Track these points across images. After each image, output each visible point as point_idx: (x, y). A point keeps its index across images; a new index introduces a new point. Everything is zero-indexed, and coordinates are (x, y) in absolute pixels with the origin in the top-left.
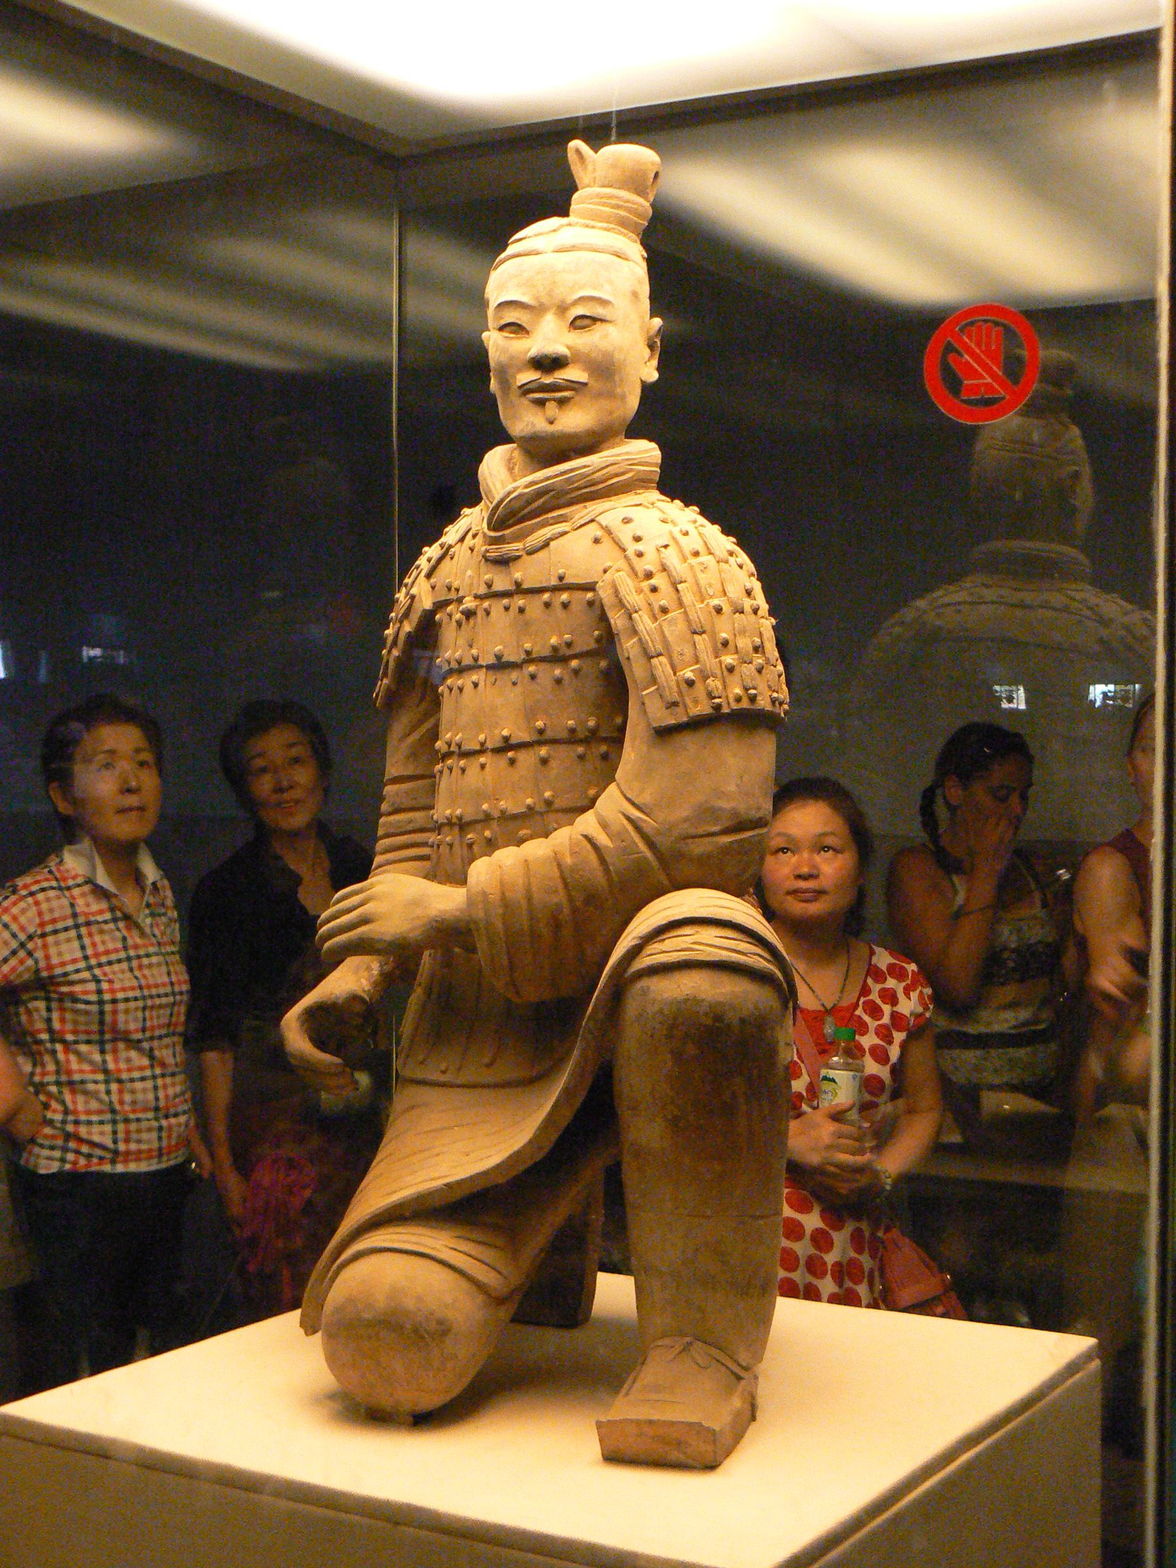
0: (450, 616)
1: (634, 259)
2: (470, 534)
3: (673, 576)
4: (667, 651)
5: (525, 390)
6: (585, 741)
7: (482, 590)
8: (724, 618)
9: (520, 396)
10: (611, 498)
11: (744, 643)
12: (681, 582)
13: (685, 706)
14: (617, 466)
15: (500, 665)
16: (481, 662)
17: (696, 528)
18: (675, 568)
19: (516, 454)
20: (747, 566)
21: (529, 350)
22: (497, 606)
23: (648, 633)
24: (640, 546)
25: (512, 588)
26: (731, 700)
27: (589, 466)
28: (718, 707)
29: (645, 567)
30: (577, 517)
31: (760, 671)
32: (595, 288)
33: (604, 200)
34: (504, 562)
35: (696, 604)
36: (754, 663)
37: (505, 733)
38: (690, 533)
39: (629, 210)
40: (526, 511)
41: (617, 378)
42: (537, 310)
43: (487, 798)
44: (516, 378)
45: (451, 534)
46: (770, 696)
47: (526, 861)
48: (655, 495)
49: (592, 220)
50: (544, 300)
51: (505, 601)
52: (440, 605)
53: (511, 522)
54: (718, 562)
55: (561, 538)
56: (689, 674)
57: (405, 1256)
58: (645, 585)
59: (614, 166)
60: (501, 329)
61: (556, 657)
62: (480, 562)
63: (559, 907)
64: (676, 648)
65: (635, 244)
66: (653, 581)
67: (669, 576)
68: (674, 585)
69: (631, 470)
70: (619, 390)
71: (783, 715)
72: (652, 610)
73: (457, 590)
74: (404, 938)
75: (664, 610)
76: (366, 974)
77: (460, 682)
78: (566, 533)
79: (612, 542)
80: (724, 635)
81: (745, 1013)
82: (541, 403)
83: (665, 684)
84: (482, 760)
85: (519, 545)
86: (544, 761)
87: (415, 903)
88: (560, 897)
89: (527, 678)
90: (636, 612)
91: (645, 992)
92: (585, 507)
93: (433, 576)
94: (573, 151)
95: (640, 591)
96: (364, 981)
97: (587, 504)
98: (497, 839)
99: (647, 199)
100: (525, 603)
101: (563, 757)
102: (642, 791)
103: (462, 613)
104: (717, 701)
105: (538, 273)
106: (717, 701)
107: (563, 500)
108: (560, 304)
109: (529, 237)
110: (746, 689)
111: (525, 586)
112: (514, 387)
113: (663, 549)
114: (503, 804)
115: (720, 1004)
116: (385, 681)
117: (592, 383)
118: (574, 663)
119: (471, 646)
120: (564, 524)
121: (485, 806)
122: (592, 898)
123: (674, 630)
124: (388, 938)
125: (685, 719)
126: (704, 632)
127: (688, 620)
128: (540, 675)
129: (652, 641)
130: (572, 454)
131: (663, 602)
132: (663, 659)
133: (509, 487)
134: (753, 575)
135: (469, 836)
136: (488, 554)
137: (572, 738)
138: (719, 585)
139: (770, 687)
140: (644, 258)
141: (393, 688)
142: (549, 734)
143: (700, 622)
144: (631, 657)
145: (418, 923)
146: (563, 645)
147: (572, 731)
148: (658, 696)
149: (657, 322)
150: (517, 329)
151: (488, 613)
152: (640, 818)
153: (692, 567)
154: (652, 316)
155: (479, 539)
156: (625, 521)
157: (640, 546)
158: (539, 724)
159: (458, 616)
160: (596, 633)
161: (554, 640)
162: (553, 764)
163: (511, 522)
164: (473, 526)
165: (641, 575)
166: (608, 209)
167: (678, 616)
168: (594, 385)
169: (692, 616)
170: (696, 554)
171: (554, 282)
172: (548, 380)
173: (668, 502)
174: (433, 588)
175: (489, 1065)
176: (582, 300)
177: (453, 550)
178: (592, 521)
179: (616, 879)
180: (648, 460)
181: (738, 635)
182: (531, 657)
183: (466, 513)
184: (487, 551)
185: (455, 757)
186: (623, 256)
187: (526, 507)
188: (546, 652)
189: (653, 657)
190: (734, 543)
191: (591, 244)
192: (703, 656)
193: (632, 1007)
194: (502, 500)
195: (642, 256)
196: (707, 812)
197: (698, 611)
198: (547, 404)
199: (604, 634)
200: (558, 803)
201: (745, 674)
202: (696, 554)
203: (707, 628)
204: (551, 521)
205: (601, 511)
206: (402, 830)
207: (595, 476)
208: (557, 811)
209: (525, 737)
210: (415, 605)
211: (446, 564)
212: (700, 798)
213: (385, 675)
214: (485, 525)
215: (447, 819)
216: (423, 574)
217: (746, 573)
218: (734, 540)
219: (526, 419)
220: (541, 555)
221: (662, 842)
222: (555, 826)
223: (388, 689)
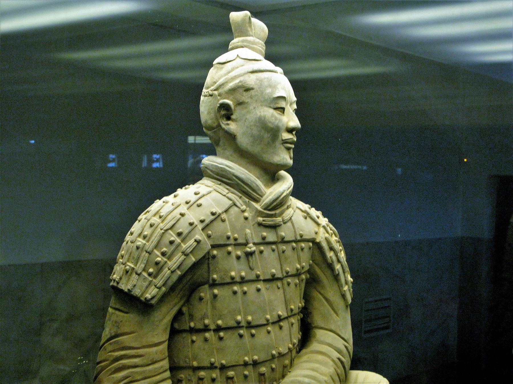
5: (285, 142)
9: (281, 144)
15: (273, 279)
34: (274, 227)
43: (274, 348)
51: (274, 247)
73: (236, 239)
111: (286, 239)
112: (280, 138)
151: (261, 252)
159: (239, 253)
194: (280, 196)
206: (157, 373)
211: (218, 225)
216: (200, 227)
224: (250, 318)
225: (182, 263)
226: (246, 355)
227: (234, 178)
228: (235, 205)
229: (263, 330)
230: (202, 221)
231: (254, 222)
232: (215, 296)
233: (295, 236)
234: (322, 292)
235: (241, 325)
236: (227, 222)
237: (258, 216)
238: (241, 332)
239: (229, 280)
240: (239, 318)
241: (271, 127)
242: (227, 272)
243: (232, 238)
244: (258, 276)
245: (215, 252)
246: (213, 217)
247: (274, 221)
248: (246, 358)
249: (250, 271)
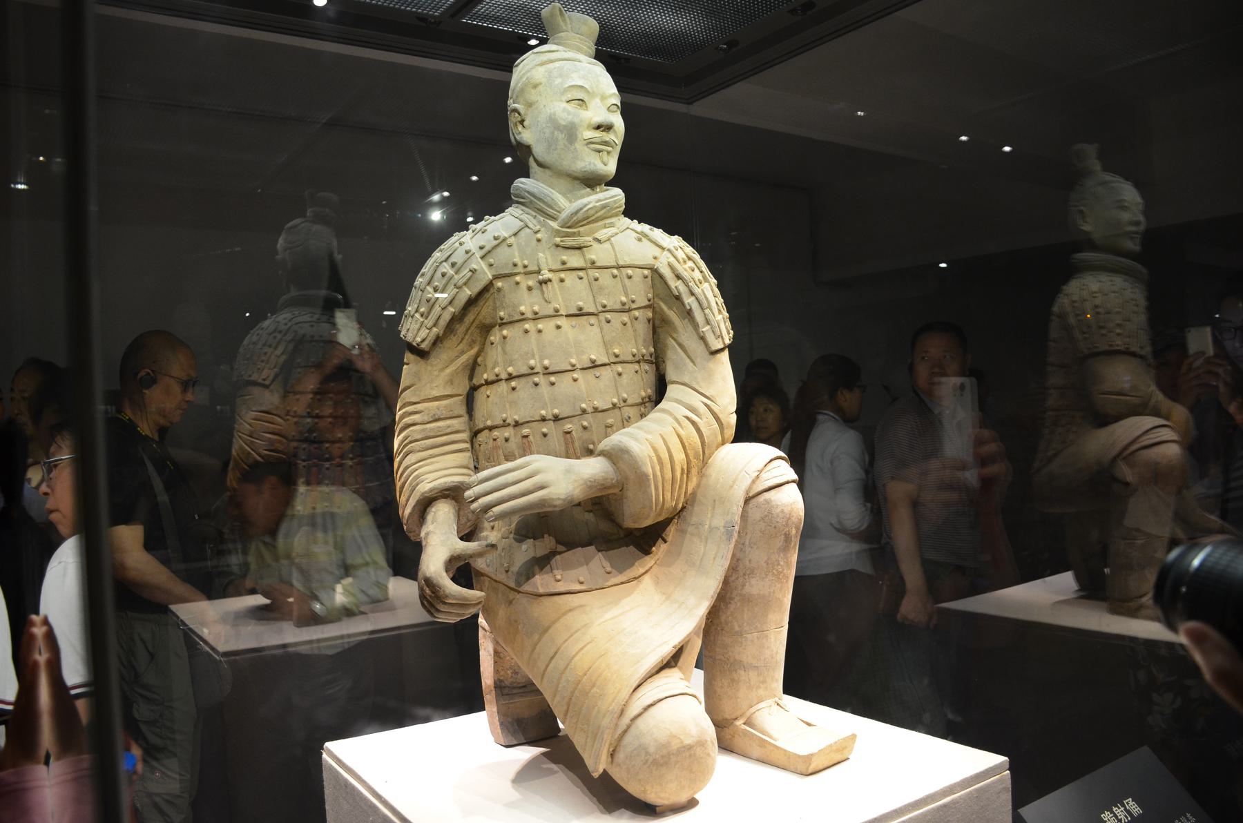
5: (590, 142)
6: (638, 362)
7: (558, 266)
15: (580, 313)
22: (570, 278)
37: (593, 357)
43: (584, 401)
51: (581, 273)
52: (497, 277)
61: (624, 309)
73: (525, 267)
78: (617, 234)
82: (599, 151)
91: (768, 502)
98: (591, 426)
111: (598, 264)
116: (435, 329)
124: (563, 497)
128: (612, 321)
142: (621, 358)
144: (693, 308)
145: (576, 484)
151: (562, 281)
159: (530, 283)
162: (624, 376)
164: (531, 225)
178: (628, 228)
184: (562, 241)
188: (618, 306)
194: (581, 209)
200: (630, 401)
204: (607, 226)
206: (441, 433)
208: (628, 406)
211: (503, 252)
216: (478, 254)
220: (607, 245)
224: (546, 362)
225: (454, 298)
226: (543, 409)
227: (527, 194)
228: (527, 226)
229: (568, 376)
230: (481, 248)
231: (550, 245)
232: (505, 338)
234: (675, 335)
235: (535, 371)
236: (515, 246)
237: (555, 237)
238: (536, 379)
239: (517, 317)
240: (532, 362)
241: (563, 125)
242: (515, 306)
243: (520, 264)
244: (557, 311)
245: (499, 284)
246: (496, 242)
248: (543, 412)
249: (546, 304)
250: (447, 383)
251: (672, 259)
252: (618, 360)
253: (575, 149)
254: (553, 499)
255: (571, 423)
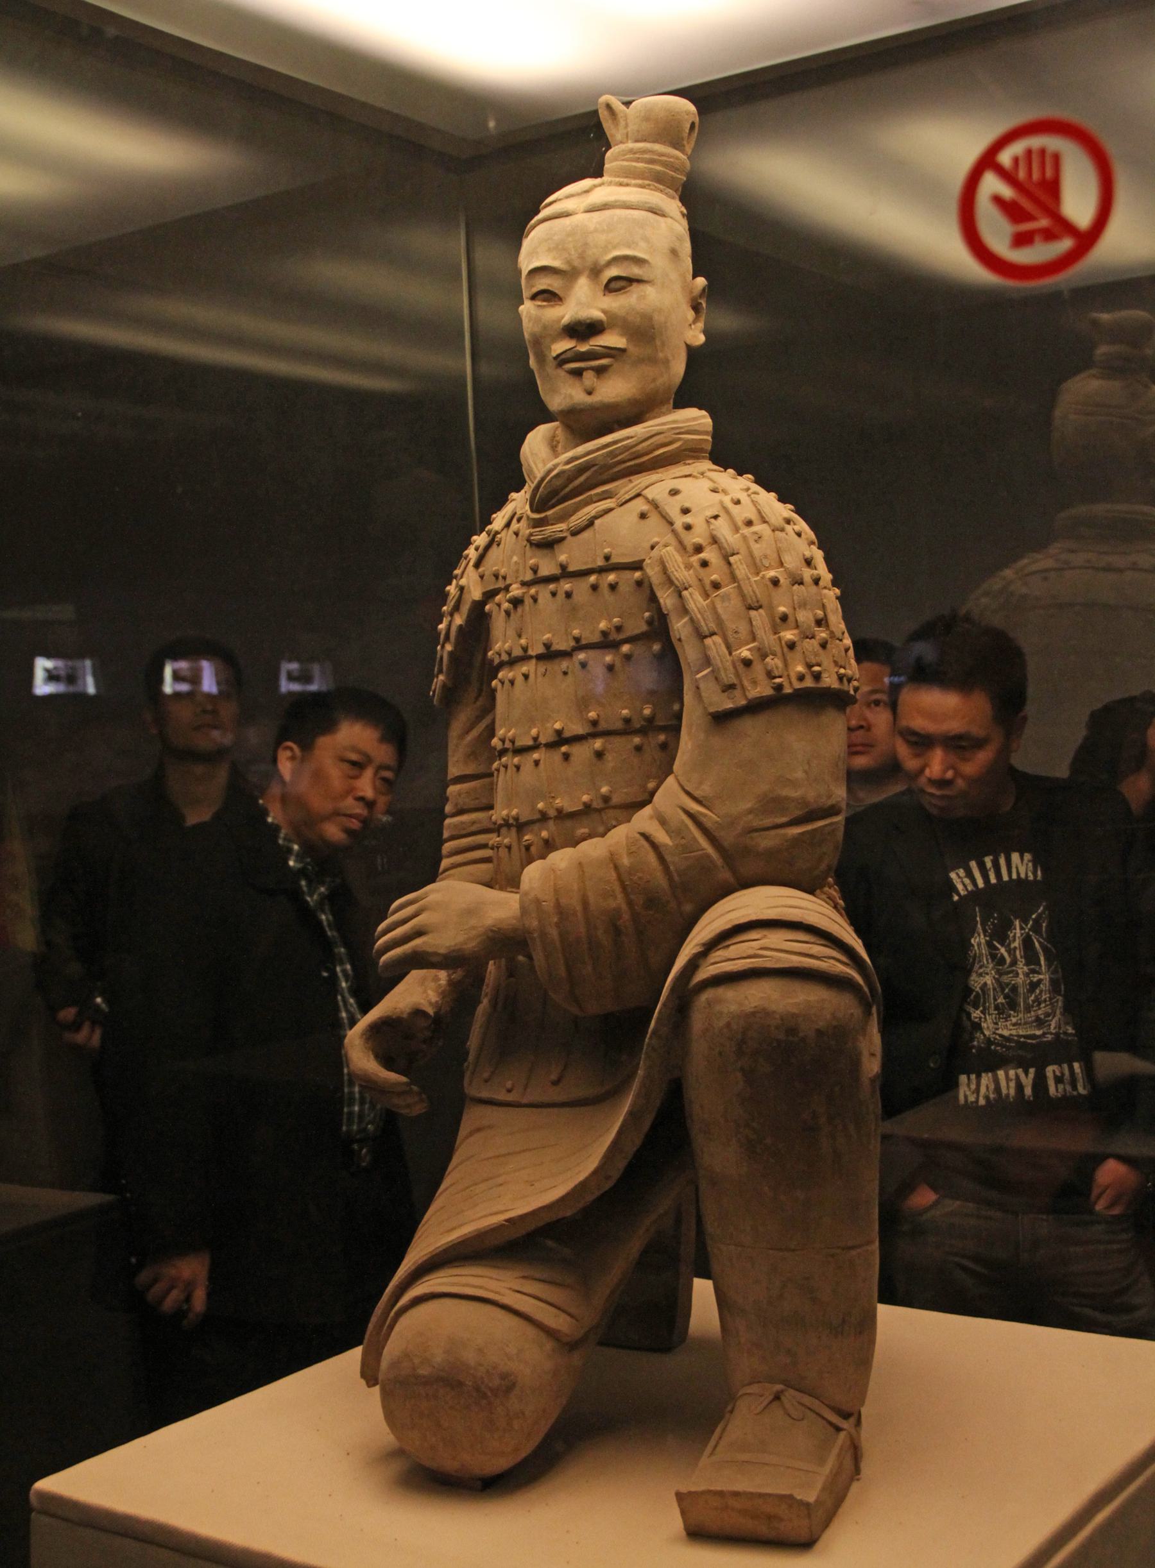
0: (499, 605)
1: (671, 215)
2: (515, 520)
3: (725, 549)
4: (721, 629)
5: (561, 360)
6: (642, 731)
7: (529, 576)
8: (780, 590)
10: (658, 471)
11: (805, 617)
12: (733, 555)
13: (743, 688)
14: (662, 435)
15: (550, 655)
16: (531, 652)
17: (749, 496)
18: (727, 541)
19: (559, 432)
20: (806, 534)
21: (563, 317)
22: (544, 592)
23: (700, 612)
24: (688, 519)
25: (557, 571)
26: (794, 680)
27: (632, 437)
28: (779, 687)
29: (694, 540)
30: (622, 492)
31: (824, 645)
32: (629, 247)
33: (637, 156)
35: (750, 576)
36: (818, 637)
37: (558, 726)
38: (742, 501)
39: (665, 164)
40: (567, 490)
41: (658, 343)
42: (569, 275)
44: (551, 349)
45: (499, 520)
46: (837, 672)
47: (580, 863)
48: (707, 465)
49: (626, 177)
50: (577, 263)
51: (552, 587)
52: (489, 595)
53: (554, 501)
54: (773, 531)
55: (606, 516)
56: (745, 653)
57: (464, 1302)
58: (695, 559)
59: (647, 119)
60: (534, 297)
61: (607, 643)
62: (525, 546)
63: (618, 910)
64: (730, 626)
65: (673, 201)
66: (702, 555)
67: (721, 548)
68: (726, 557)
69: (679, 439)
70: (661, 355)
71: (852, 692)
72: (703, 586)
74: (459, 950)
75: (716, 586)
76: (433, 985)
77: (511, 675)
78: (611, 510)
79: (659, 516)
80: (782, 609)
81: (821, 1024)
82: (578, 373)
83: (720, 665)
84: (536, 756)
85: (562, 526)
86: (599, 755)
87: (470, 912)
88: (620, 901)
89: (578, 666)
90: (686, 589)
92: (630, 481)
93: (482, 564)
94: (604, 107)
95: (689, 567)
96: (430, 992)
97: (632, 478)
98: (554, 840)
99: (683, 152)
100: (571, 587)
101: (620, 749)
102: (701, 783)
103: (510, 601)
104: (778, 680)
105: (568, 235)
106: (778, 680)
107: (605, 477)
108: (592, 267)
109: (560, 200)
110: (809, 666)
111: (571, 569)
113: (713, 521)
114: (558, 802)
115: (794, 1016)
116: (441, 677)
117: (632, 349)
118: (625, 648)
119: (520, 636)
120: (609, 501)
121: (540, 805)
122: (652, 901)
123: (728, 607)
124: (442, 951)
125: (744, 702)
126: (761, 607)
127: (743, 596)
128: (591, 663)
129: (704, 620)
130: (616, 426)
131: (714, 577)
132: (717, 639)
133: (549, 465)
134: (813, 543)
135: (526, 838)
136: (532, 538)
137: (627, 728)
138: (775, 555)
139: (836, 663)
140: (683, 215)
141: (450, 685)
142: (603, 726)
143: (756, 596)
144: (683, 638)
145: (474, 932)
146: (613, 629)
147: (627, 721)
148: (714, 679)
149: (701, 281)
150: (549, 296)
152: (699, 812)
153: (744, 538)
154: (694, 277)
155: (524, 522)
156: (672, 493)
157: (688, 519)
158: (592, 715)
160: (647, 614)
161: (603, 625)
162: (609, 757)
163: (554, 501)
165: (690, 548)
166: (640, 165)
167: (731, 590)
168: (632, 349)
169: (747, 590)
170: (749, 523)
171: (586, 244)
172: (584, 348)
173: (721, 472)
174: (482, 577)
175: (555, 1083)
176: (617, 260)
177: (499, 536)
178: (638, 495)
179: (676, 878)
180: (697, 428)
181: (797, 609)
182: (580, 644)
183: (513, 498)
184: (531, 534)
185: (510, 754)
186: (658, 212)
187: (566, 486)
188: (596, 638)
189: (706, 637)
190: (792, 511)
191: (624, 202)
192: (760, 633)
193: (698, 1021)
194: (543, 479)
195: (682, 213)
196: (771, 803)
197: (754, 584)
198: (584, 373)
199: (656, 617)
200: (615, 800)
201: (807, 649)
202: (749, 523)
203: (764, 602)
205: (647, 483)
206: (464, 832)
207: (639, 447)
208: (615, 807)
209: (579, 729)
210: (465, 596)
211: (494, 552)
212: (764, 787)
213: (440, 671)
214: (528, 507)
215: (504, 820)
216: (471, 563)
217: (806, 542)
218: (792, 507)
219: (563, 391)
220: (586, 535)
221: (728, 838)
222: (614, 823)
223: (444, 686)
233: (594, 561)
237: (529, 528)
247: (543, 533)
250: (470, 755)
251: (671, 553)
252: (596, 731)
253: (548, 375)
254: (428, 952)
255: (532, 831)
